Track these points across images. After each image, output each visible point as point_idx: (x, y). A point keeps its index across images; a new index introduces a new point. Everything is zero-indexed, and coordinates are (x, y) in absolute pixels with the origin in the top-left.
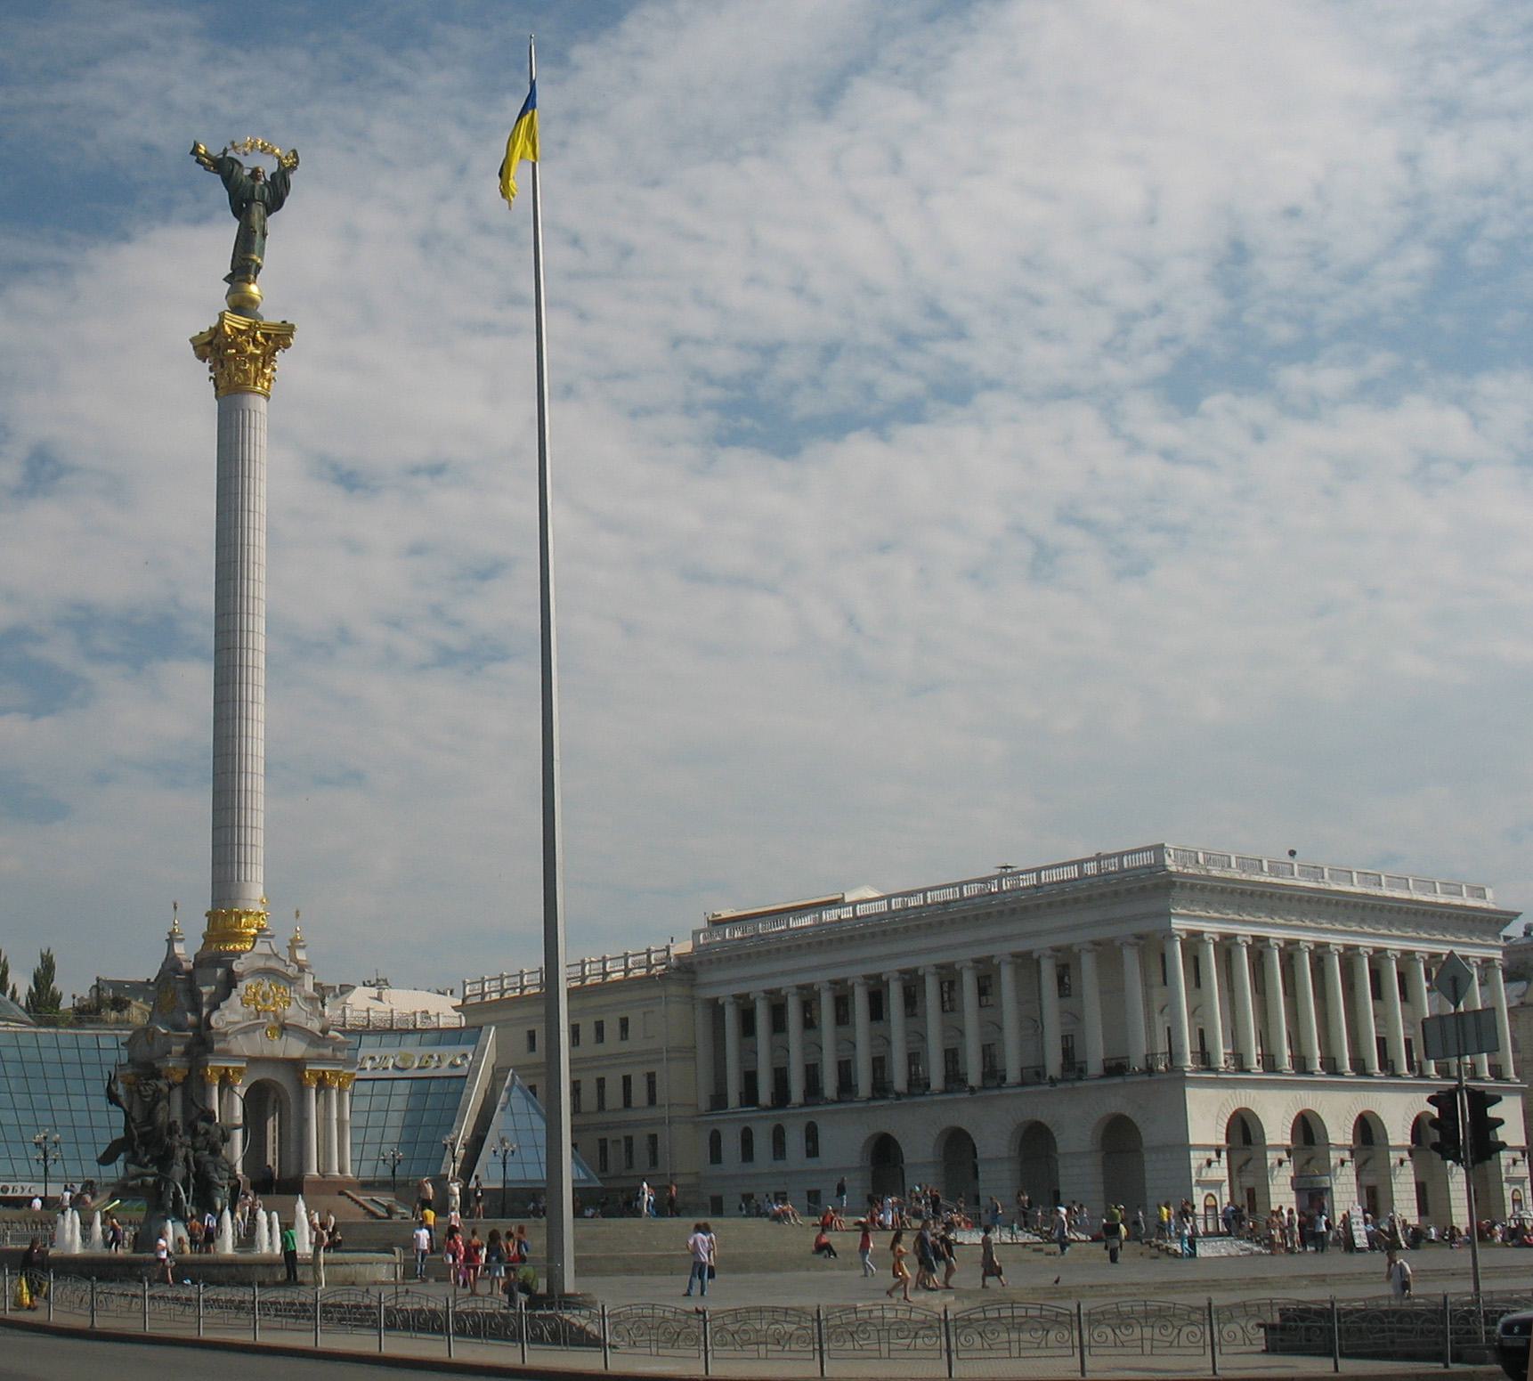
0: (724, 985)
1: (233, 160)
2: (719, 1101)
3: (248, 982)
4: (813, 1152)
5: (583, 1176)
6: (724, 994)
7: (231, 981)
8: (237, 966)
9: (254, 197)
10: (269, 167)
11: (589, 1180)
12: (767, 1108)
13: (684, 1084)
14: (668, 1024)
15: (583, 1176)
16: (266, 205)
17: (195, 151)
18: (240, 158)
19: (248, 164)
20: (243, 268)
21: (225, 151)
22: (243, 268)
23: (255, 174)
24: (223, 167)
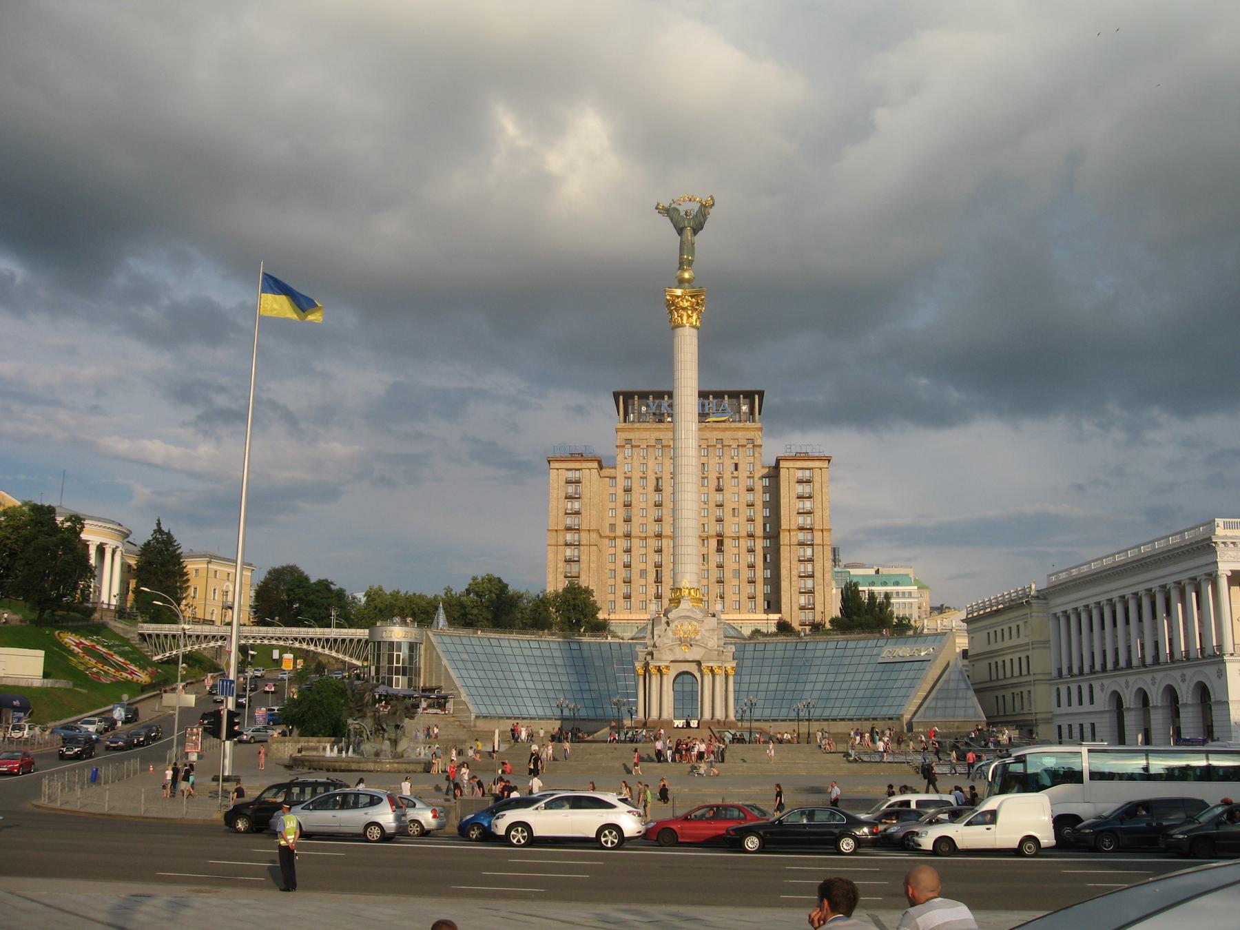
0: (1062, 604)
2: (1060, 670)
4: (1092, 702)
6: (1059, 610)
13: (1044, 663)
14: (1036, 625)
19: (682, 209)
24: (669, 212)
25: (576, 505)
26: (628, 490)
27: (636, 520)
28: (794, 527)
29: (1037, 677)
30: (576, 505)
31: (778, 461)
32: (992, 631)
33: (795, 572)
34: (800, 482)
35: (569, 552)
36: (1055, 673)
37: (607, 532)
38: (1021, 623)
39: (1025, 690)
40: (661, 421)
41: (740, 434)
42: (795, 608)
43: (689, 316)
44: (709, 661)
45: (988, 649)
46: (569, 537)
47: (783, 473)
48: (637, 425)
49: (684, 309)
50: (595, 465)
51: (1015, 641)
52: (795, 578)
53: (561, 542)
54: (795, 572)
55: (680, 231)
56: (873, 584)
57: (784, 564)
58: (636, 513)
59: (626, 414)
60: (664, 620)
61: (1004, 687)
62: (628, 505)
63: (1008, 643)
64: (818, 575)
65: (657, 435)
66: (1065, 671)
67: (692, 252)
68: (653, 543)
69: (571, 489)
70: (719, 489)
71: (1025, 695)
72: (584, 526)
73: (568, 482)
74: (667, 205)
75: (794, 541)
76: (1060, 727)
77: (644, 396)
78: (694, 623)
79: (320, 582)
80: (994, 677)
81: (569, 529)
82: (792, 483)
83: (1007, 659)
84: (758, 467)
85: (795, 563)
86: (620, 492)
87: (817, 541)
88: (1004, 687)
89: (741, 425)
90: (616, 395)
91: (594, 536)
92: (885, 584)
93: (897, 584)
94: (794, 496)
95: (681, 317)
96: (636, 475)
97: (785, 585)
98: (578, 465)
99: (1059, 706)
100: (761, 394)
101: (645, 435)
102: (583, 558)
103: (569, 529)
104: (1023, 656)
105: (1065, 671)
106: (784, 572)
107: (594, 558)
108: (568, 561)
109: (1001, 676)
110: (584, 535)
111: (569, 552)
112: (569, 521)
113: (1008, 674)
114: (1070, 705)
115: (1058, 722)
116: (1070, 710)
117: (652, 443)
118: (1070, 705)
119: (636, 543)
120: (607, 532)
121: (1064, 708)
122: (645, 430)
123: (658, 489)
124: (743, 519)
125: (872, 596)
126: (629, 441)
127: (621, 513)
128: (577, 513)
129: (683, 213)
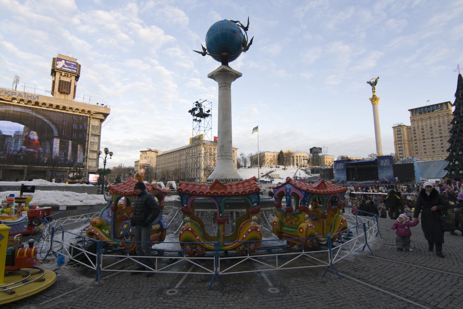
9: (373, 84)
10: (374, 80)
25: (400, 136)
26: (414, 130)
27: (417, 137)
30: (400, 136)
35: (400, 146)
37: (410, 140)
40: (421, 114)
41: (444, 113)
46: (399, 142)
58: (417, 135)
62: (415, 133)
67: (375, 89)
68: (422, 141)
69: (399, 133)
70: (440, 126)
77: (416, 109)
81: (399, 141)
86: (412, 131)
90: (409, 110)
96: (416, 127)
102: (403, 146)
103: (399, 141)
108: (399, 147)
110: (403, 142)
111: (400, 146)
112: (399, 139)
119: (418, 142)
120: (410, 140)
123: (422, 129)
126: (413, 120)
127: (413, 136)
128: (401, 137)
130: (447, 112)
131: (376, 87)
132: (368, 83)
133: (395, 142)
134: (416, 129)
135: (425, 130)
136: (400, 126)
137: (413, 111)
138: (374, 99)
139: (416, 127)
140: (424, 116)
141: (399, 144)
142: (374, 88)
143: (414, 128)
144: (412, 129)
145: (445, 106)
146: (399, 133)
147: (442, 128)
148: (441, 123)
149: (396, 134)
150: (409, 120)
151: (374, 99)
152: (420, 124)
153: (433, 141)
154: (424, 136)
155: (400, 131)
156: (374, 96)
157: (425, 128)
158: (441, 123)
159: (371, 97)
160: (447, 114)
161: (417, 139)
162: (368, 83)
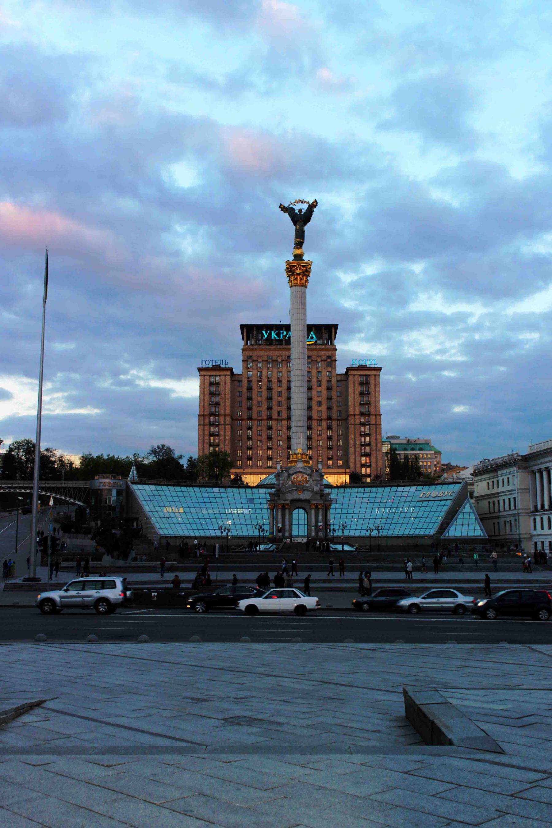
1: (292, 208)
2: (536, 507)
3: (294, 476)
5: (482, 535)
7: (289, 475)
8: (291, 472)
9: (301, 218)
10: (305, 207)
11: (484, 536)
12: (547, 510)
13: (524, 502)
15: (482, 535)
16: (303, 221)
17: (280, 207)
18: (294, 207)
19: (297, 208)
20: (299, 244)
21: (289, 205)
22: (299, 244)
23: (300, 211)
25: (217, 399)
26: (250, 389)
27: (255, 409)
28: (357, 412)
29: (520, 511)
30: (217, 399)
31: (348, 369)
32: (490, 481)
33: (358, 442)
34: (361, 384)
36: (532, 509)
38: (510, 476)
39: (513, 519)
41: (323, 353)
42: (358, 465)
43: (301, 279)
44: (315, 500)
45: (489, 492)
47: (351, 378)
48: (256, 347)
49: (298, 274)
50: (229, 373)
51: (506, 488)
52: (358, 446)
53: (207, 422)
54: (358, 442)
55: (295, 224)
56: (405, 449)
57: (352, 436)
59: (248, 339)
60: (286, 474)
61: (498, 517)
62: (250, 399)
63: (501, 489)
64: (373, 444)
65: (269, 353)
66: (539, 507)
69: (214, 389)
71: (513, 522)
72: (222, 412)
73: (211, 384)
74: (286, 206)
75: (358, 421)
76: (536, 543)
77: (260, 328)
78: (305, 476)
79: (98, 457)
80: (492, 511)
82: (357, 385)
83: (501, 499)
84: (334, 375)
85: (358, 436)
86: (244, 390)
87: (373, 422)
88: (498, 517)
89: (323, 347)
90: (242, 327)
91: (228, 419)
92: (413, 449)
93: (421, 449)
94: (357, 393)
95: (296, 279)
96: (255, 379)
97: (352, 450)
98: (218, 373)
99: (535, 529)
100: (336, 326)
101: (261, 353)
102: (222, 433)
103: (211, 414)
104: (512, 497)
105: (539, 507)
106: (351, 442)
107: (228, 433)
109: (496, 510)
110: (222, 419)
112: (213, 409)
113: (502, 509)
114: (542, 529)
115: (535, 539)
116: (543, 532)
117: (265, 358)
118: (542, 529)
121: (539, 531)
122: (261, 350)
123: (270, 389)
124: (323, 408)
125: (406, 457)
126: (250, 357)
127: (245, 404)
128: (217, 404)
129: (297, 211)
130: (330, 353)
131: (306, 228)
132: (283, 209)
133: (201, 416)
134: (255, 387)
135: (275, 394)
136: (217, 368)
137: (249, 331)
138: (298, 272)
139: (255, 379)
140: (277, 353)
141: (211, 424)
142: (303, 232)
143: (250, 381)
144: (245, 383)
145: (326, 335)
146: (214, 389)
147: (314, 393)
148: (314, 380)
149: (207, 392)
150: (239, 356)
151: (298, 272)
152: (264, 372)
153: (270, 428)
154: (270, 408)
155: (218, 384)
156: (298, 257)
157: (275, 386)
158: (314, 380)
159: (291, 258)
160: (329, 357)
161: (255, 416)
162: (283, 209)
